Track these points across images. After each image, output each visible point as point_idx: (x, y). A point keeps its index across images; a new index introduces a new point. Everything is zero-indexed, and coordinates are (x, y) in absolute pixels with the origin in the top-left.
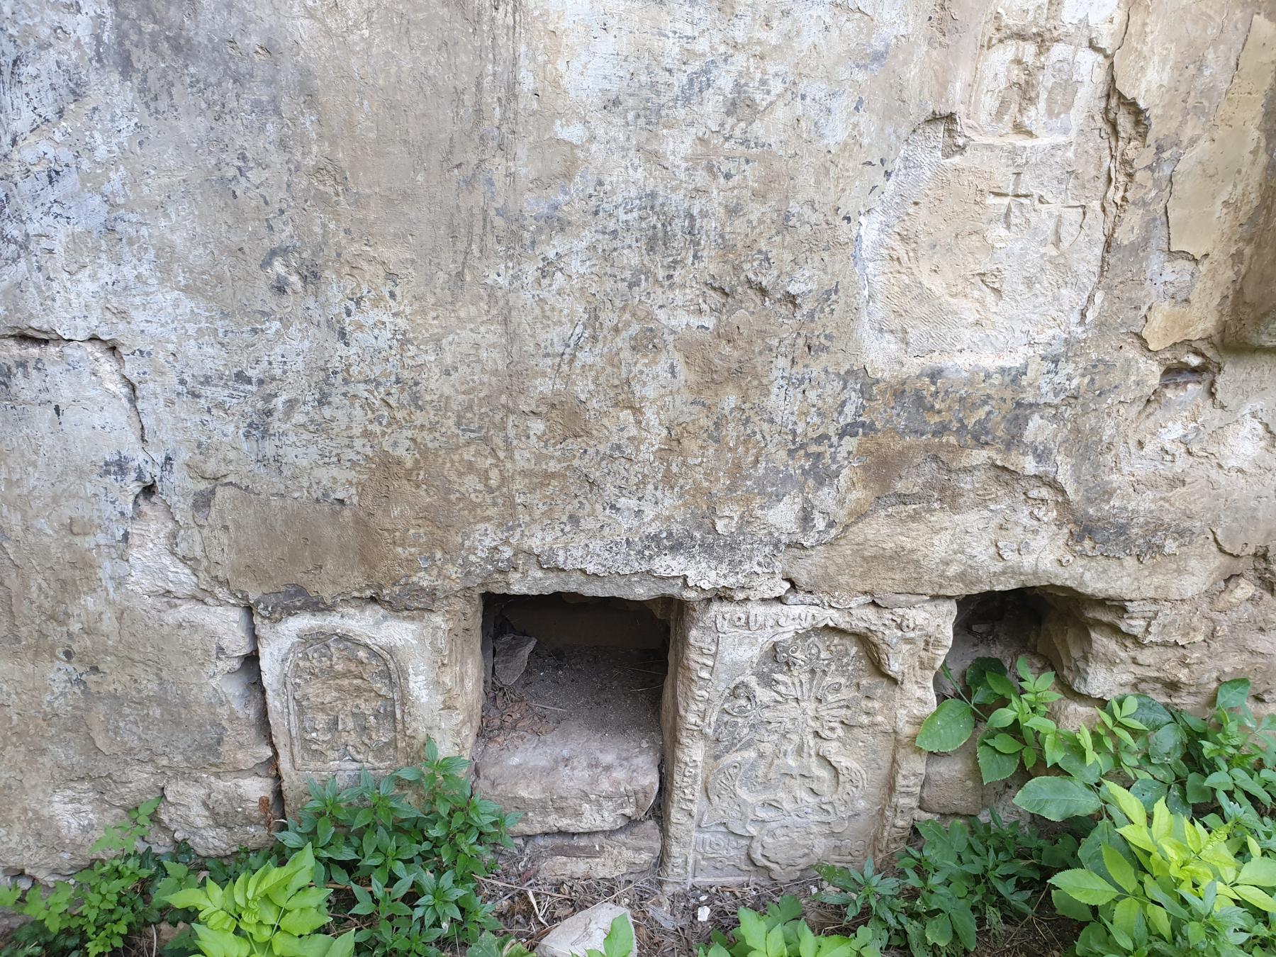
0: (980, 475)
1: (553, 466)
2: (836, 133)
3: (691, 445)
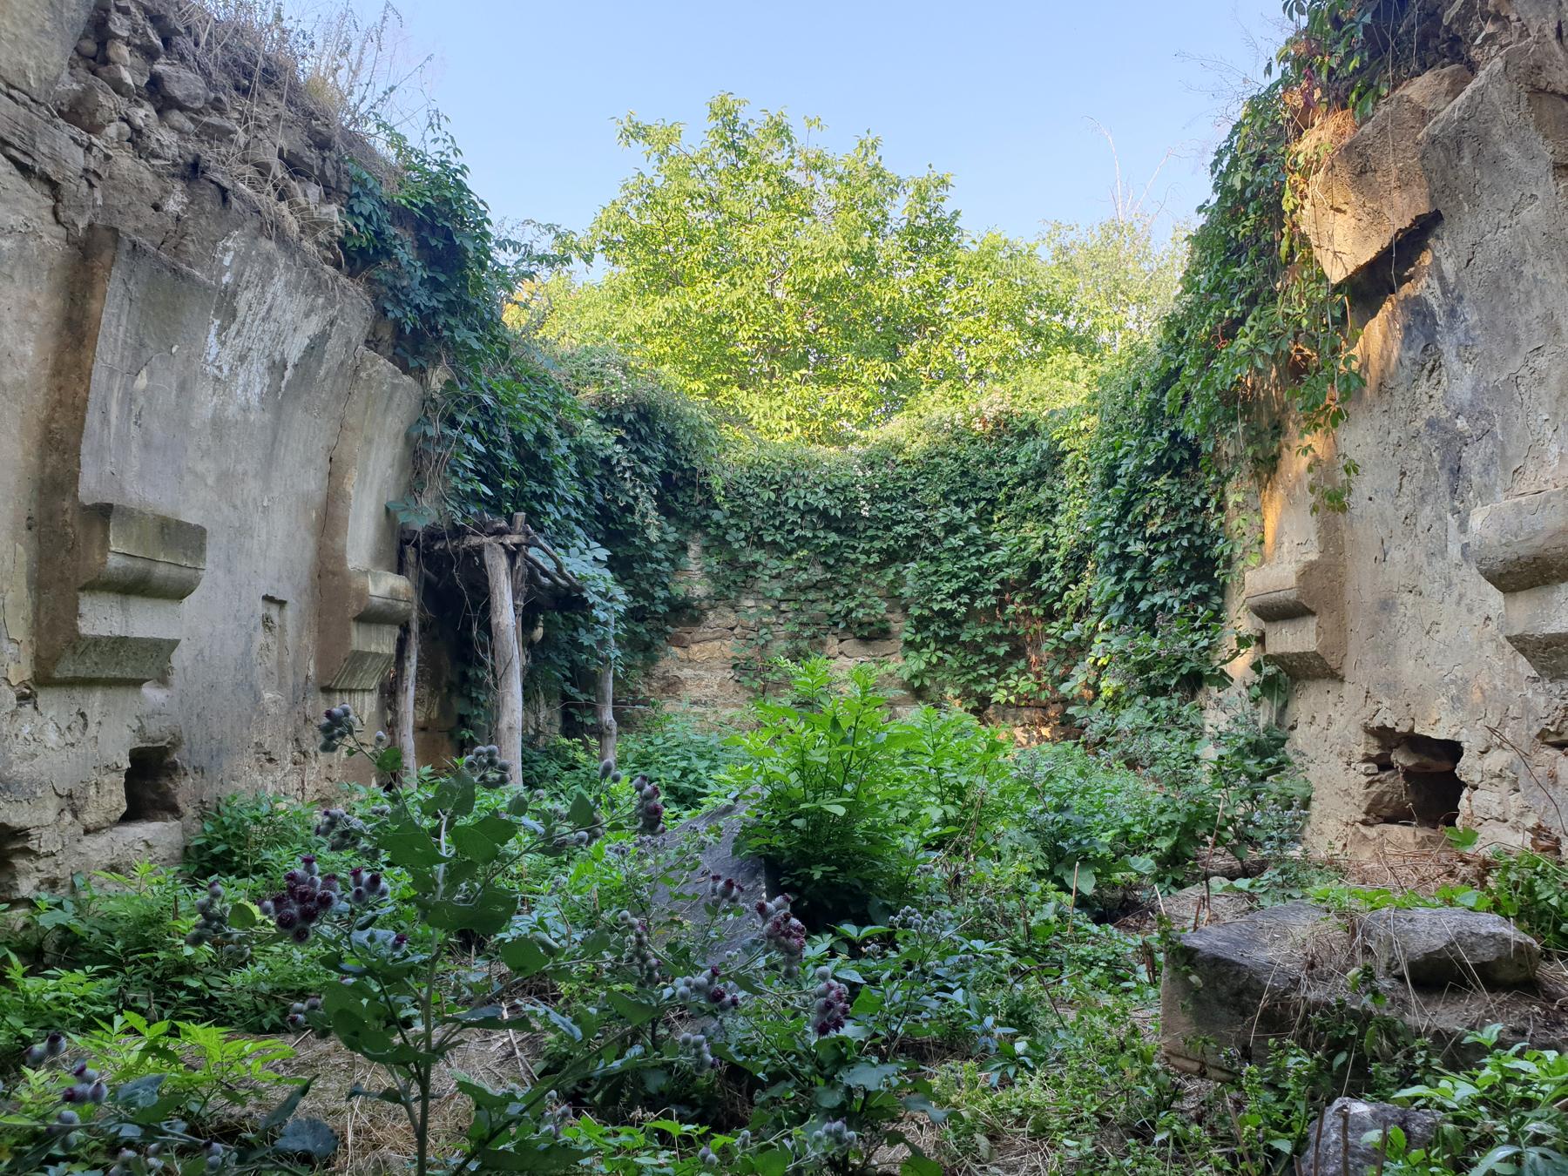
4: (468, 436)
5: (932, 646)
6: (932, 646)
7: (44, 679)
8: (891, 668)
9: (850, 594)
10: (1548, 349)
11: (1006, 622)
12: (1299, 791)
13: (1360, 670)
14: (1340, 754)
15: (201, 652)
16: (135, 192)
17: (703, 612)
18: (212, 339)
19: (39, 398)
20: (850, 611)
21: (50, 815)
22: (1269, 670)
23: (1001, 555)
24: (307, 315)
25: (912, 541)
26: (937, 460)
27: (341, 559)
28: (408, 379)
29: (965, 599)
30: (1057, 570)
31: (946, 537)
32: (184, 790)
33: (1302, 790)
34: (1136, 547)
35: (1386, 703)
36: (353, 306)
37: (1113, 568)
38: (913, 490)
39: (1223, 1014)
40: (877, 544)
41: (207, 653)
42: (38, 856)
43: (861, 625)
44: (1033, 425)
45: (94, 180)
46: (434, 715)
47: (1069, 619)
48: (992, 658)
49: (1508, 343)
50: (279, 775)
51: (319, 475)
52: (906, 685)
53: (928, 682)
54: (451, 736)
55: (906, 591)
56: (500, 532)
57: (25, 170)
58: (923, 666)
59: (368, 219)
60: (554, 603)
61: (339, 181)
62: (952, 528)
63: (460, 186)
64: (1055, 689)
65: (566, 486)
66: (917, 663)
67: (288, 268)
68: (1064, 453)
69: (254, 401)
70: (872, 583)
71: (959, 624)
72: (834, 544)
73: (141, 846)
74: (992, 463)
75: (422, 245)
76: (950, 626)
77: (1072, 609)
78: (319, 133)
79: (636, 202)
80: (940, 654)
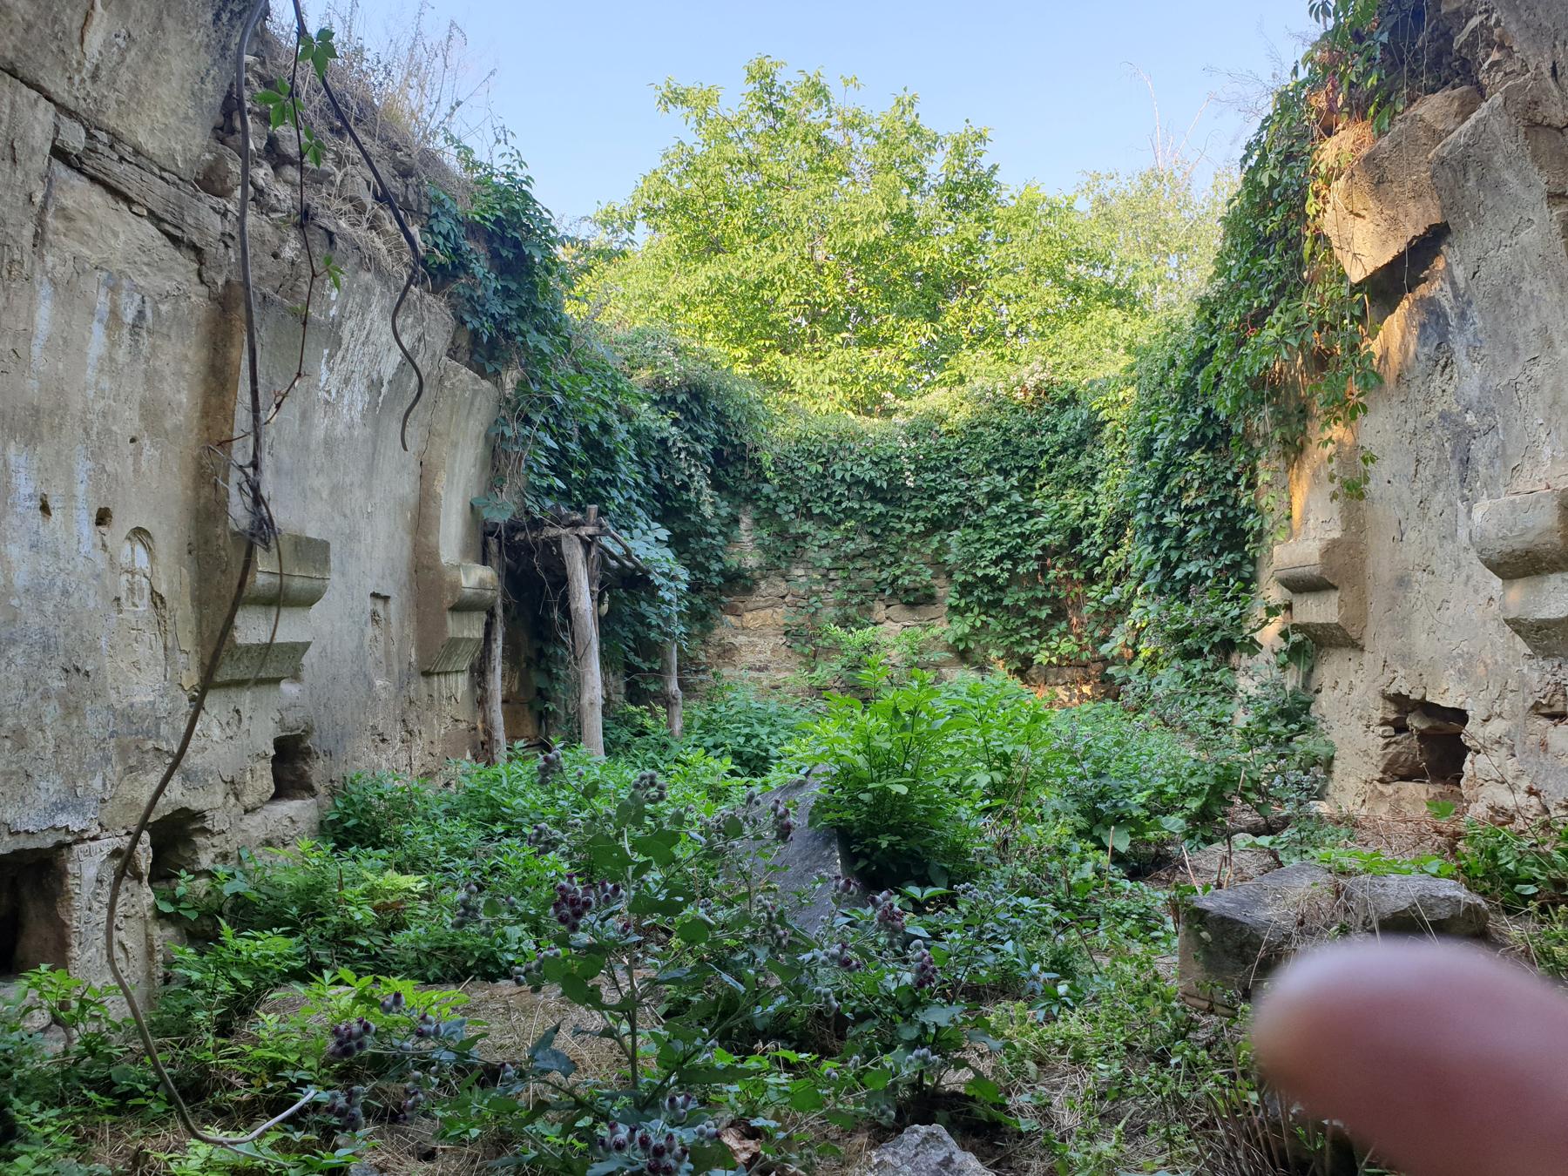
0: (151, 754)
1: (14, 767)
2: (91, 604)
3: (64, 747)
4: (541, 434)
5: (976, 610)
6: (976, 610)
7: (208, 683)
8: (936, 631)
9: (897, 562)
10: (1543, 360)
11: (1047, 587)
12: (1322, 751)
13: (1379, 644)
14: (1360, 718)
15: (324, 649)
16: (258, 245)
17: (755, 582)
18: (323, 367)
19: (193, 438)
20: (897, 578)
21: (219, 799)
22: (1296, 637)
23: (1043, 521)
25: (956, 510)
26: (979, 429)
27: (434, 554)
28: (486, 384)
29: (1008, 564)
30: (1097, 536)
31: (989, 505)
32: (317, 771)
33: (1326, 749)
34: (1172, 519)
35: (1402, 672)
36: (433, 322)
37: (1150, 537)
38: (957, 460)
39: (1229, 963)
40: (922, 514)
42: (212, 834)
43: (907, 591)
44: (1073, 393)
45: (230, 242)
46: (515, 688)
47: (1108, 583)
48: (1034, 621)
49: (1509, 351)
50: (391, 753)
51: (413, 478)
52: (951, 648)
53: (972, 646)
54: (531, 708)
55: (951, 558)
56: (575, 525)
57: (175, 241)
58: (967, 630)
59: (446, 238)
60: (625, 583)
61: (420, 203)
62: (994, 496)
63: (526, 196)
64: (1095, 650)
65: (628, 471)
66: (962, 627)
68: (1104, 423)
69: (357, 418)
70: (917, 551)
71: (1001, 589)
72: (880, 514)
73: (286, 822)
74: (1034, 432)
75: (495, 255)
76: (993, 590)
77: (1111, 573)
78: (402, 163)
79: (676, 170)
80: (983, 617)
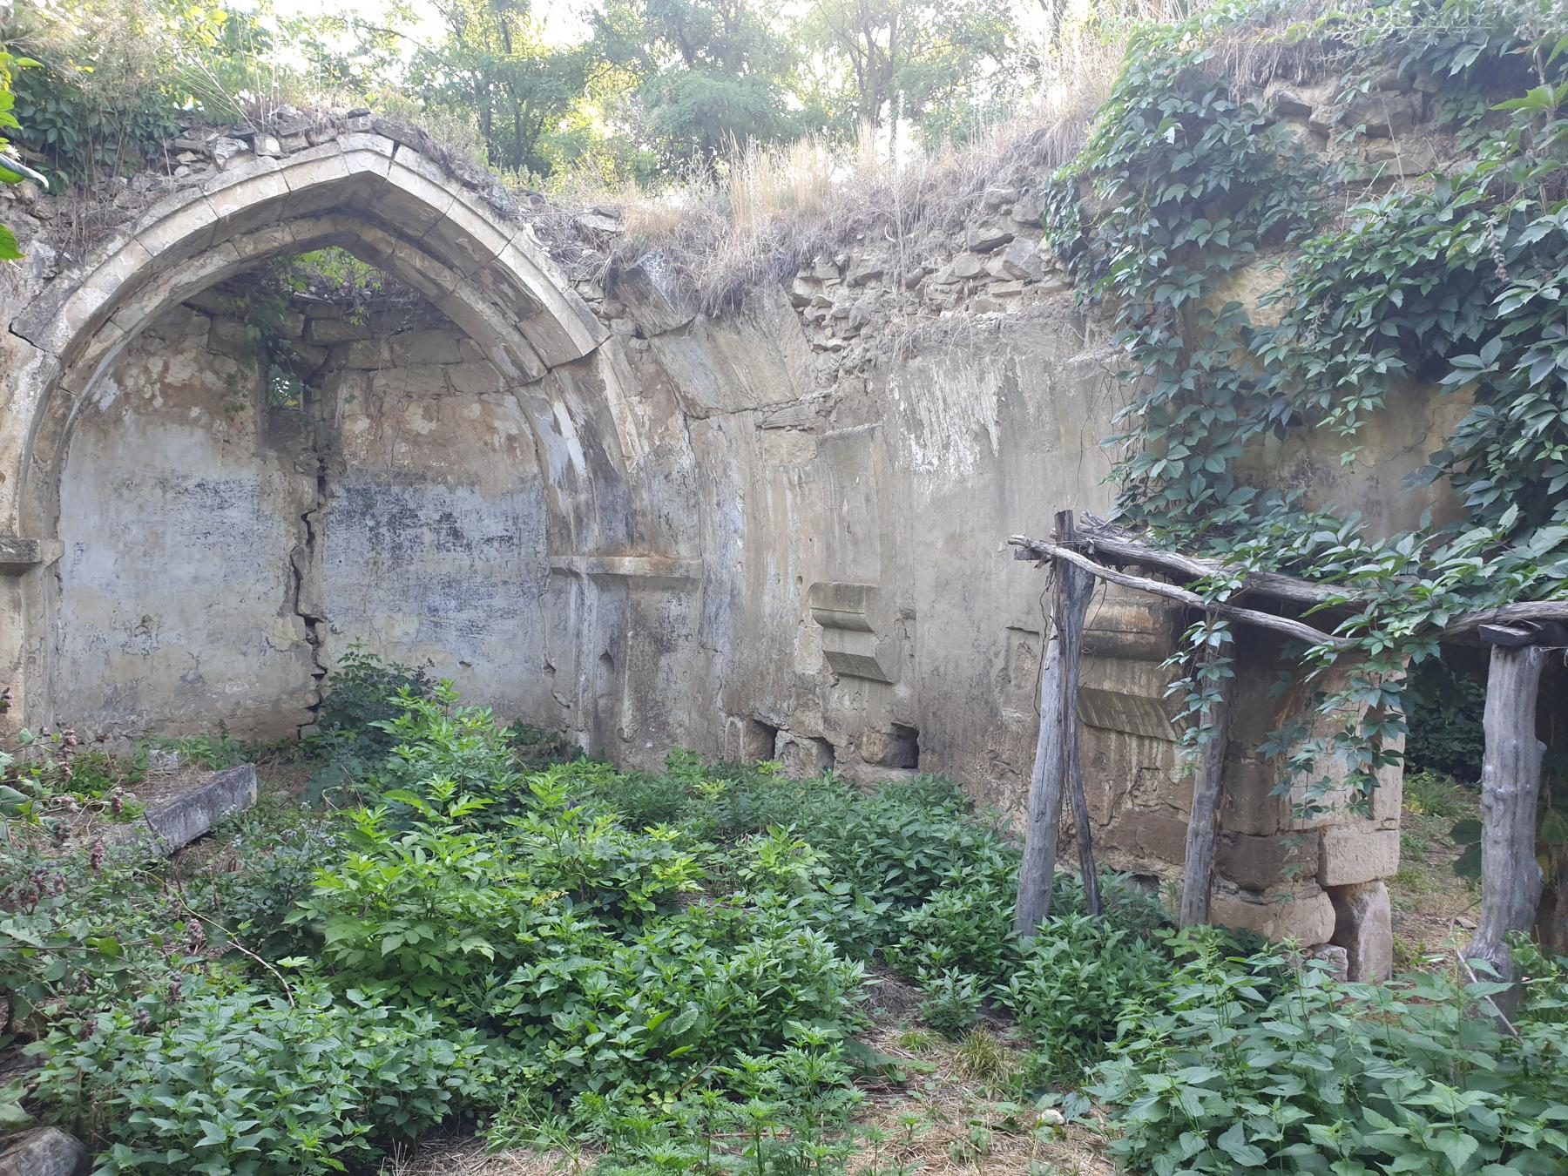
15: (937, 668)
18: (915, 448)
24: (981, 379)
41: (942, 670)
67: (938, 363)
